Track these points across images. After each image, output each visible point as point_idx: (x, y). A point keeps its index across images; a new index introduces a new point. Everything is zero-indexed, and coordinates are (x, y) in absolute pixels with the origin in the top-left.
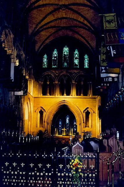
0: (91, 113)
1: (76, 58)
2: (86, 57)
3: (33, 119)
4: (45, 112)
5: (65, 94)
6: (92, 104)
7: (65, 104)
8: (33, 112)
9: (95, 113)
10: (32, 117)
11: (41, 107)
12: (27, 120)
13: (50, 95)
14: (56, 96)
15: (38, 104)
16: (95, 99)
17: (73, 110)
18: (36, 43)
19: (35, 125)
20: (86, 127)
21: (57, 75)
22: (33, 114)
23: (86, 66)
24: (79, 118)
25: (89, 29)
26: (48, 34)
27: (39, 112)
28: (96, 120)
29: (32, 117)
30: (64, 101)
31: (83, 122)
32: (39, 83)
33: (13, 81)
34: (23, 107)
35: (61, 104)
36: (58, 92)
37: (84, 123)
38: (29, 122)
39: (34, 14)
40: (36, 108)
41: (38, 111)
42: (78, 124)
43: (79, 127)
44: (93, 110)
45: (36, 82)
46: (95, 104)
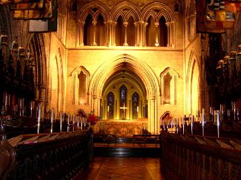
0: (173, 78)
6: (175, 61)
7: (127, 61)
9: (182, 78)
13: (99, 45)
14: (110, 47)
17: (141, 72)
19: (70, 99)
20: (165, 103)
24: (152, 85)
27: (77, 76)
30: (125, 55)
32: (77, 21)
34: (47, 63)
36: (112, 39)
37: (161, 95)
40: (72, 69)
41: (76, 74)
43: (152, 103)
45: (72, 20)
46: (181, 61)
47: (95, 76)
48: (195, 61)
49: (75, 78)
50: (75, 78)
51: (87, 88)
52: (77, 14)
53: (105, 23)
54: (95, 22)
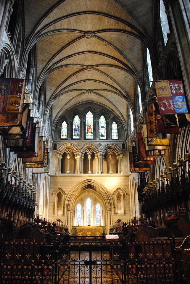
1: (102, 127)
2: (114, 125)
3: (49, 204)
4: (65, 194)
5: (89, 172)
7: (91, 183)
8: (49, 194)
9: (129, 195)
10: (48, 202)
11: (60, 188)
12: (41, 205)
15: (56, 185)
16: (127, 177)
18: (55, 109)
21: (79, 148)
22: (49, 198)
23: (115, 136)
25: (119, 93)
26: (68, 98)
27: (56, 194)
28: (130, 204)
29: (48, 202)
30: (89, 179)
31: (113, 206)
33: (36, 155)
34: (39, 189)
35: (84, 184)
38: (43, 209)
39: (55, 74)
40: (53, 190)
41: (56, 193)
42: (108, 210)
43: (109, 213)
44: (126, 191)
46: (127, 183)
47: (69, 194)
48: (136, 183)
49: (55, 196)
50: (55, 196)
51: (63, 204)
52: (57, 151)
53: (75, 157)
54: (68, 157)
